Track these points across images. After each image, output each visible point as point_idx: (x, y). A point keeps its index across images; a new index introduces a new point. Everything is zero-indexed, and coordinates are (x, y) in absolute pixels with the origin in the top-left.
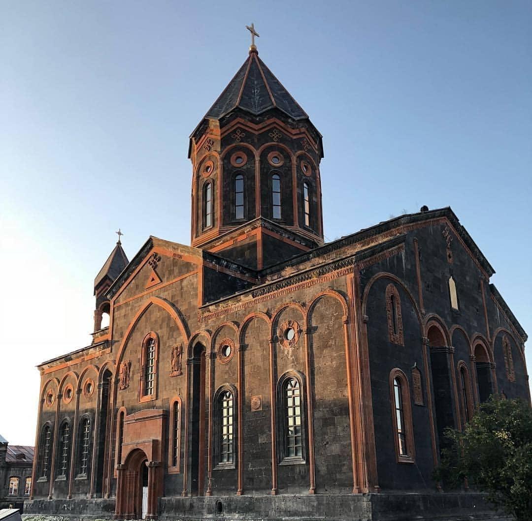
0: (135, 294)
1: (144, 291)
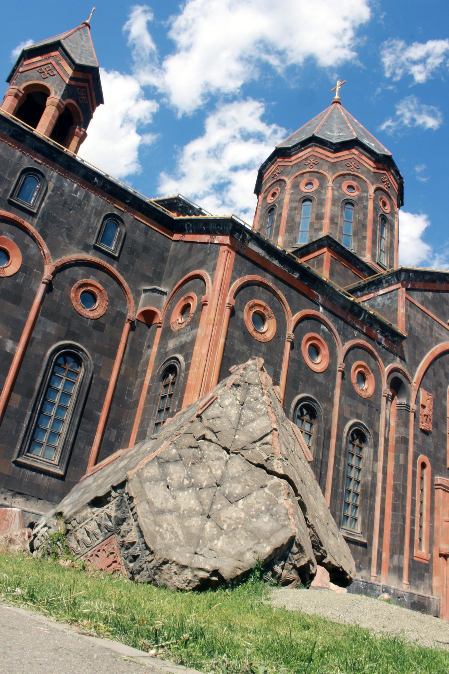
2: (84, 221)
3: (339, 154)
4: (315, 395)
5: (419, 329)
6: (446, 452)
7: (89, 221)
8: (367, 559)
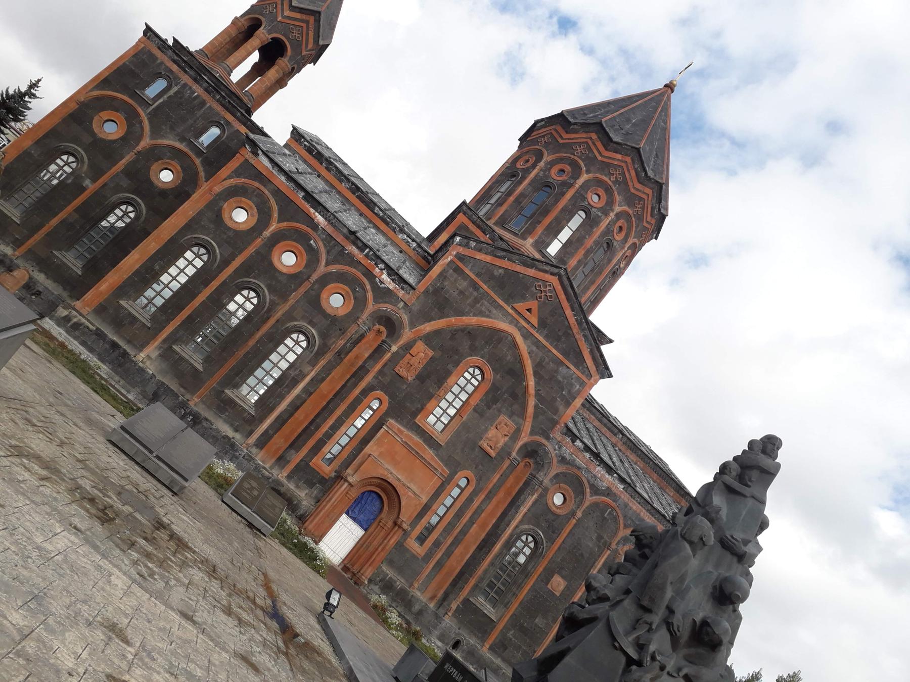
0: (492, 288)
1: (507, 301)
2: (191, 121)
3: (573, 136)
4: (269, 287)
5: (455, 294)
6: (422, 409)
7: (195, 122)
8: (249, 428)
